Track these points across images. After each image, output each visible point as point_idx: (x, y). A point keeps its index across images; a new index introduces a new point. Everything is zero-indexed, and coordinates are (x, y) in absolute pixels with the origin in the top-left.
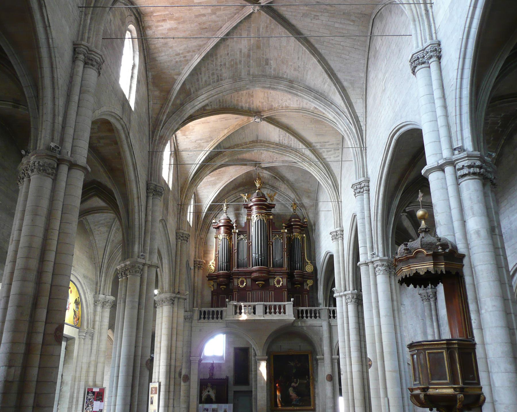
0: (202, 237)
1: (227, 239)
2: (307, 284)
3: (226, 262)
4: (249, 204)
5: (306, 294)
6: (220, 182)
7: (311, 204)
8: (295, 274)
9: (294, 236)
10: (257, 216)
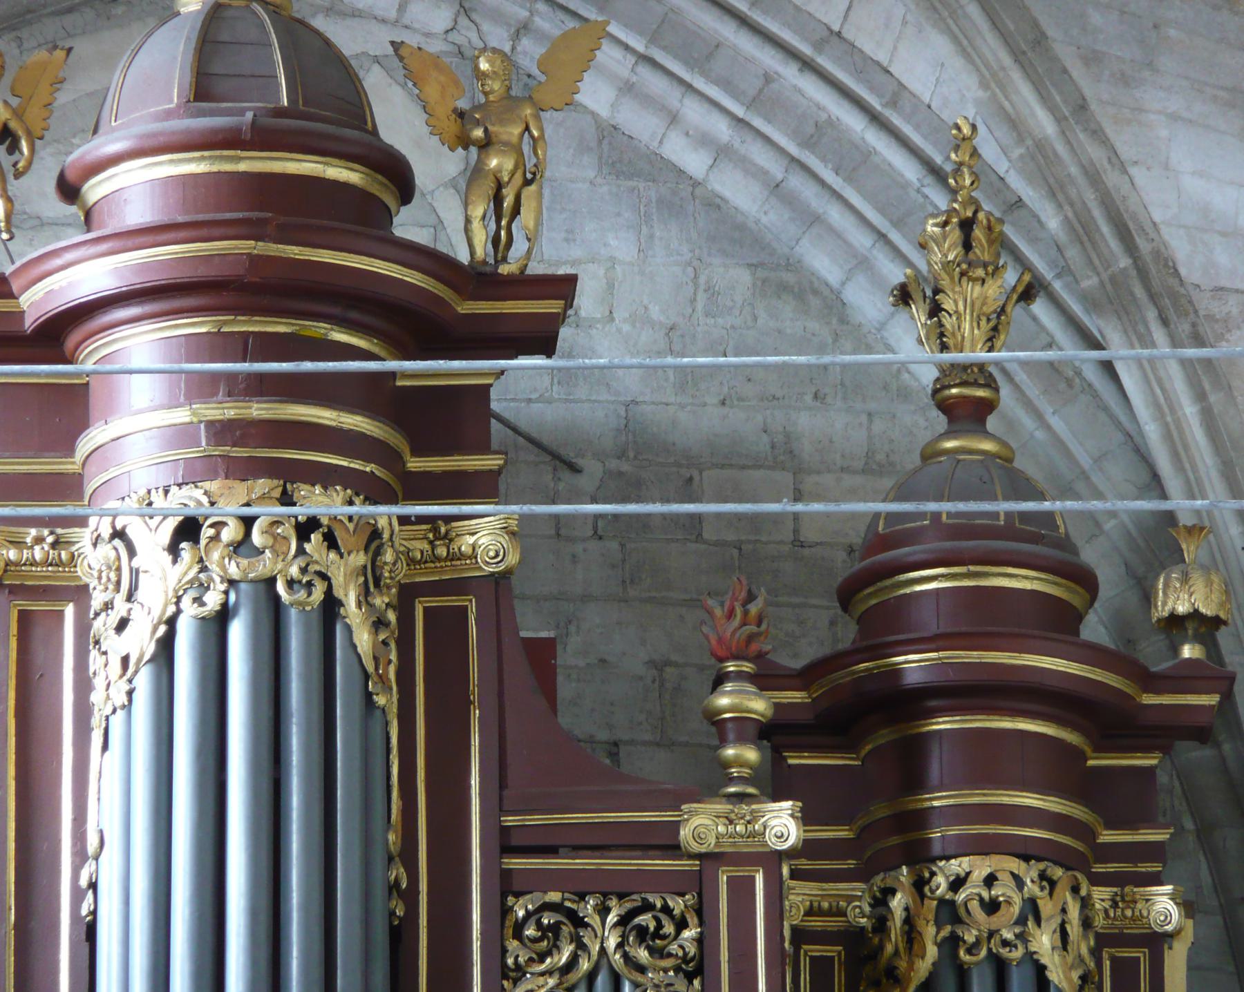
4: (37, 269)
9: (950, 912)
10: (188, 530)
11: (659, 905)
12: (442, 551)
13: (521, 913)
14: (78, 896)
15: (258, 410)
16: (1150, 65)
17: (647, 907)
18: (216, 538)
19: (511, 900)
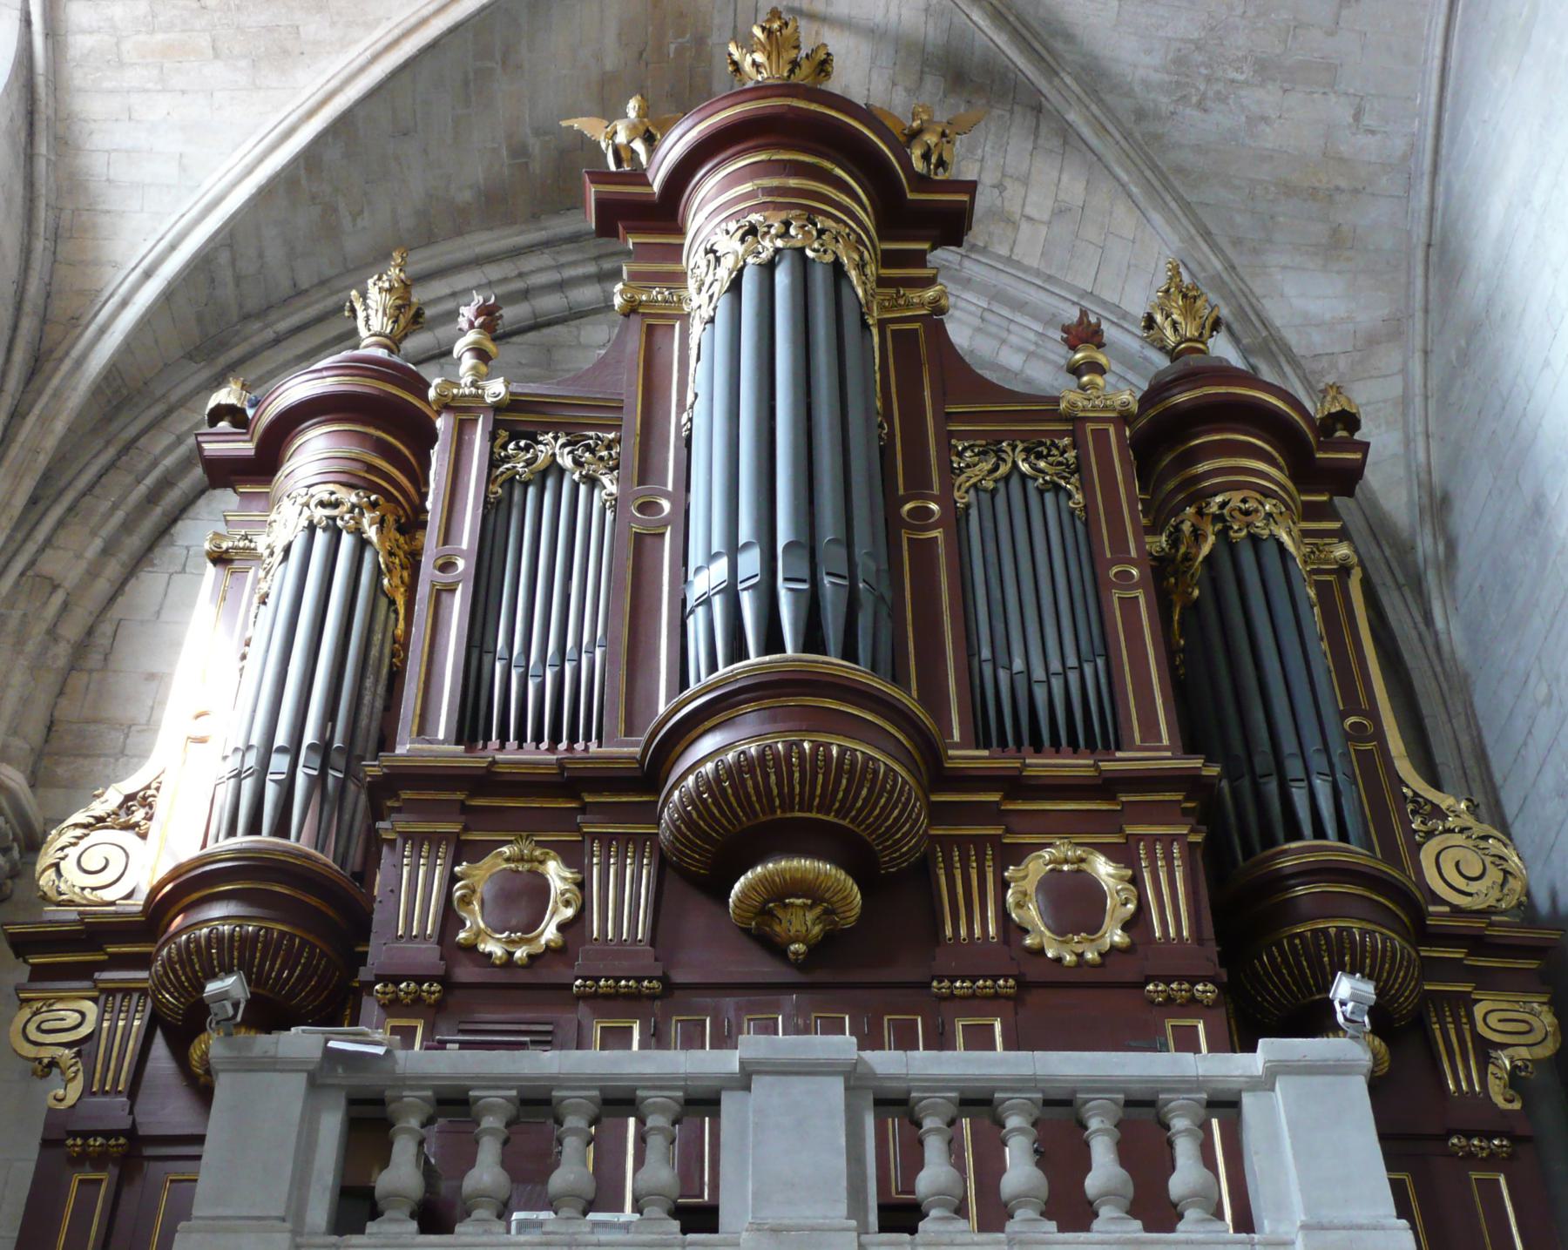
0: (52, 564)
1: (362, 544)
2: (1485, 1050)
3: (323, 747)
5: (1493, 1161)
6: (344, 44)
7: (1370, 311)
8: (1293, 854)
11: (1048, 443)
12: (902, 302)
13: (960, 448)
14: (679, 427)
15: (793, 182)
16: (1270, 241)
17: (1042, 444)
18: (768, 233)
19: (954, 442)
